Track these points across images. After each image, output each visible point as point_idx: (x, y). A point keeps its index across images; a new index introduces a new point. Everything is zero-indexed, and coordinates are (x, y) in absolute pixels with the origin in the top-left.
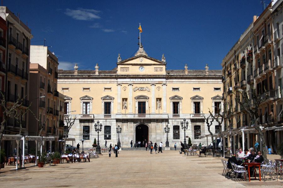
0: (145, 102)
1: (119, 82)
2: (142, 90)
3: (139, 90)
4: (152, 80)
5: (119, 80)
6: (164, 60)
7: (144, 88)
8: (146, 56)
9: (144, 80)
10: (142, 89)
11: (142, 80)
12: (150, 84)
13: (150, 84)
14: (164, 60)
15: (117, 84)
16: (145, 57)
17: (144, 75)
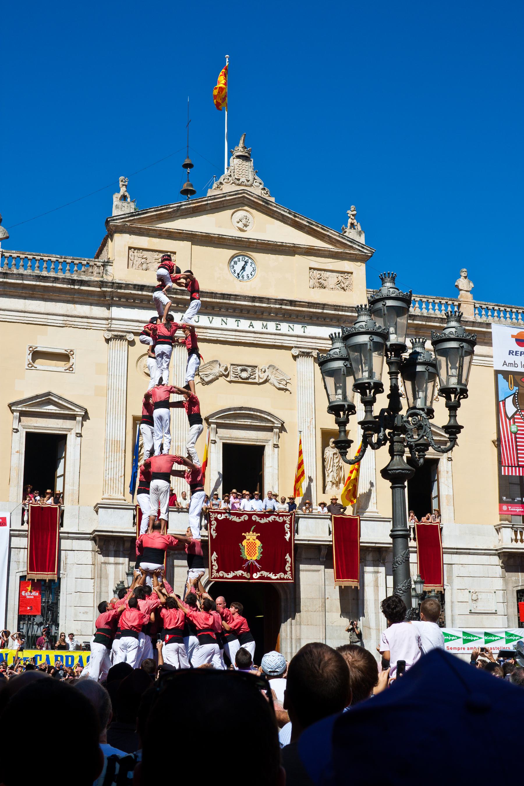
0: (262, 448)
1: (116, 325)
2: (245, 381)
3: (231, 378)
4: (298, 329)
5: (117, 312)
6: (360, 233)
7: (257, 372)
8: (267, 202)
9: (258, 325)
10: (244, 375)
11: (244, 324)
12: (289, 348)
13: (289, 348)
14: (360, 233)
15: (109, 335)
16: (264, 208)
17: (261, 299)
